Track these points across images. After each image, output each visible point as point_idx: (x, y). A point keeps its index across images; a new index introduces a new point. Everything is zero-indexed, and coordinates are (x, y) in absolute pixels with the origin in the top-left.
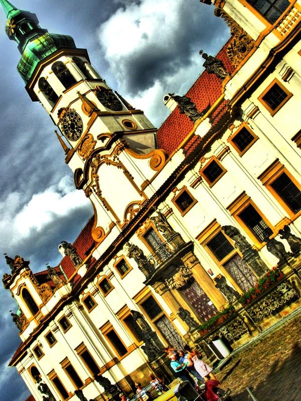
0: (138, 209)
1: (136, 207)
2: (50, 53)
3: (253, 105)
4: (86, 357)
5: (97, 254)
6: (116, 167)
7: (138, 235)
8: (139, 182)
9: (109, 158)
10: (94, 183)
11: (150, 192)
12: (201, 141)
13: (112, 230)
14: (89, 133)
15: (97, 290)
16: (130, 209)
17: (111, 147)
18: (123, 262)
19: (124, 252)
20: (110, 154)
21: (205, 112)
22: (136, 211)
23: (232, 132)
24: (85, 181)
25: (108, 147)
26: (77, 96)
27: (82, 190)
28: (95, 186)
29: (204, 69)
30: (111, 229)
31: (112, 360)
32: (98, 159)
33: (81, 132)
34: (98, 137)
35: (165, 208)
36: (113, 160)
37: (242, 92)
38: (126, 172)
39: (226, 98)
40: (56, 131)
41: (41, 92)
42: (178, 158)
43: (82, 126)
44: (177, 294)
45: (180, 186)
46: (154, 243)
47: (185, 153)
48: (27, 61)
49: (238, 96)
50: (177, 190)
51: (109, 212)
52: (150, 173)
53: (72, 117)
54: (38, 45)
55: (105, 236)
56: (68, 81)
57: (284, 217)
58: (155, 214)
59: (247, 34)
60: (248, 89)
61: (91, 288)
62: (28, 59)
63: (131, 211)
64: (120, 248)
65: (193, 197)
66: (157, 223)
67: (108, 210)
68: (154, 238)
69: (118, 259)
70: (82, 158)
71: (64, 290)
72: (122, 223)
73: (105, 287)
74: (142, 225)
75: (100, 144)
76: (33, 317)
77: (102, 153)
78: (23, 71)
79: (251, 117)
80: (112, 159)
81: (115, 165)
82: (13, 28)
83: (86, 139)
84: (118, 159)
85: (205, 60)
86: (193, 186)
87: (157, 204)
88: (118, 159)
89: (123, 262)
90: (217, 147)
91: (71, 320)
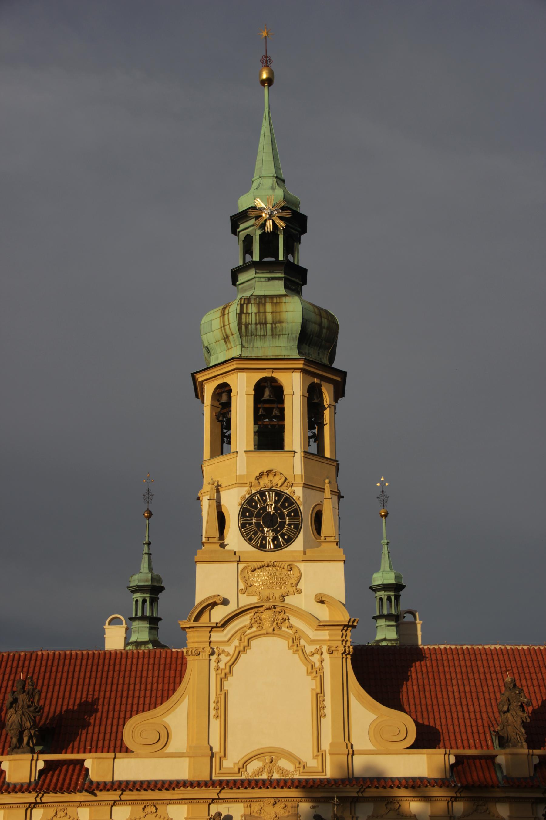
0: (288, 772)
1: (284, 763)
6: (303, 669)
9: (303, 642)
10: (230, 649)
20: (313, 638)
22: (281, 770)
28: (228, 654)
48: (273, 323)
54: (315, 323)
62: (281, 322)
70: (242, 586)
78: (247, 325)
80: (310, 649)
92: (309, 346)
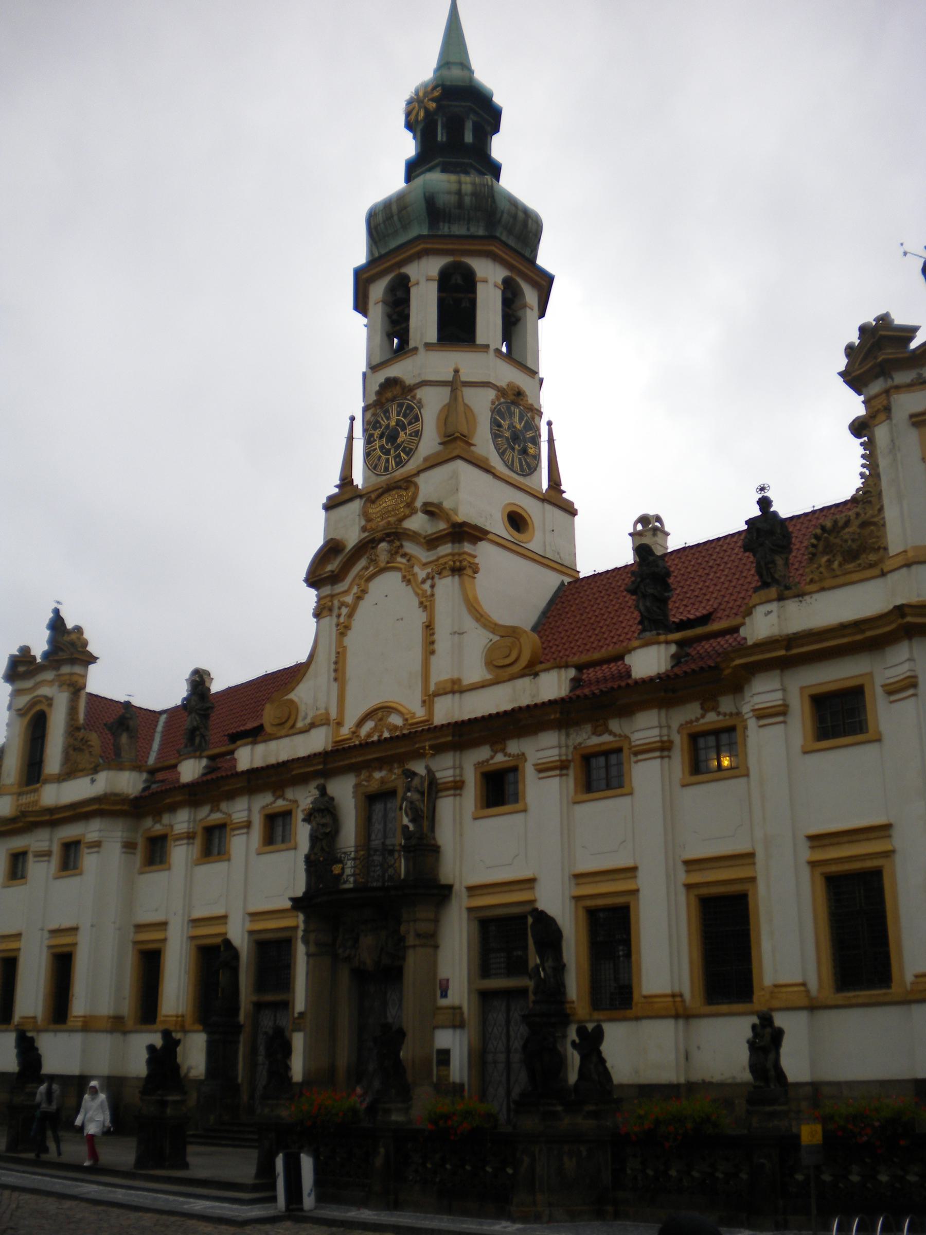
0: (396, 727)
2: (463, 231)
3: (779, 695)
4: (62, 965)
5: (248, 757)
6: (416, 602)
7: (357, 786)
8: (441, 672)
9: (416, 569)
10: (349, 599)
11: (446, 711)
12: (620, 687)
13: (314, 732)
14: (416, 479)
15: (190, 837)
16: (380, 714)
17: (436, 547)
18: (286, 815)
19: (304, 798)
20: (424, 560)
21: (683, 625)
23: (703, 716)
24: (336, 578)
25: (432, 542)
26: (450, 378)
27: (313, 592)
29: (746, 527)
30: (313, 725)
31: (109, 1017)
32: (393, 554)
33: (400, 463)
34: (426, 504)
35: (450, 772)
36: (420, 579)
37: (775, 650)
38: (429, 628)
39: (743, 632)
40: (352, 419)
41: (380, 305)
42: (552, 686)
43: (410, 452)
44: (344, 976)
45: (513, 747)
46: (377, 826)
47: (576, 683)
49: (762, 652)
50: (503, 750)
51: (335, 686)
52: (475, 672)
53: (405, 416)
54: (449, 193)
55: (291, 732)
56: (457, 326)
57: (677, 990)
58: (419, 768)
59: (884, 525)
60: (795, 651)
61: (181, 821)
62: (405, 208)
63: (381, 720)
64: (302, 780)
65: (524, 792)
66: (409, 790)
67: (336, 679)
68: (385, 816)
69: (280, 803)
70: (363, 523)
71: (128, 782)
72: (345, 731)
73: (212, 844)
74: (380, 769)
75: (417, 523)
76: (15, 789)
77: (410, 547)
78: (376, 227)
79: (762, 715)
80: (421, 574)
81: (417, 594)
82: (427, 111)
83: (400, 488)
84: (432, 586)
85: (756, 512)
86: (543, 769)
87: (439, 749)
88: (432, 586)
89: (286, 815)
90: (645, 727)
91: (89, 861)
92: (449, 222)
